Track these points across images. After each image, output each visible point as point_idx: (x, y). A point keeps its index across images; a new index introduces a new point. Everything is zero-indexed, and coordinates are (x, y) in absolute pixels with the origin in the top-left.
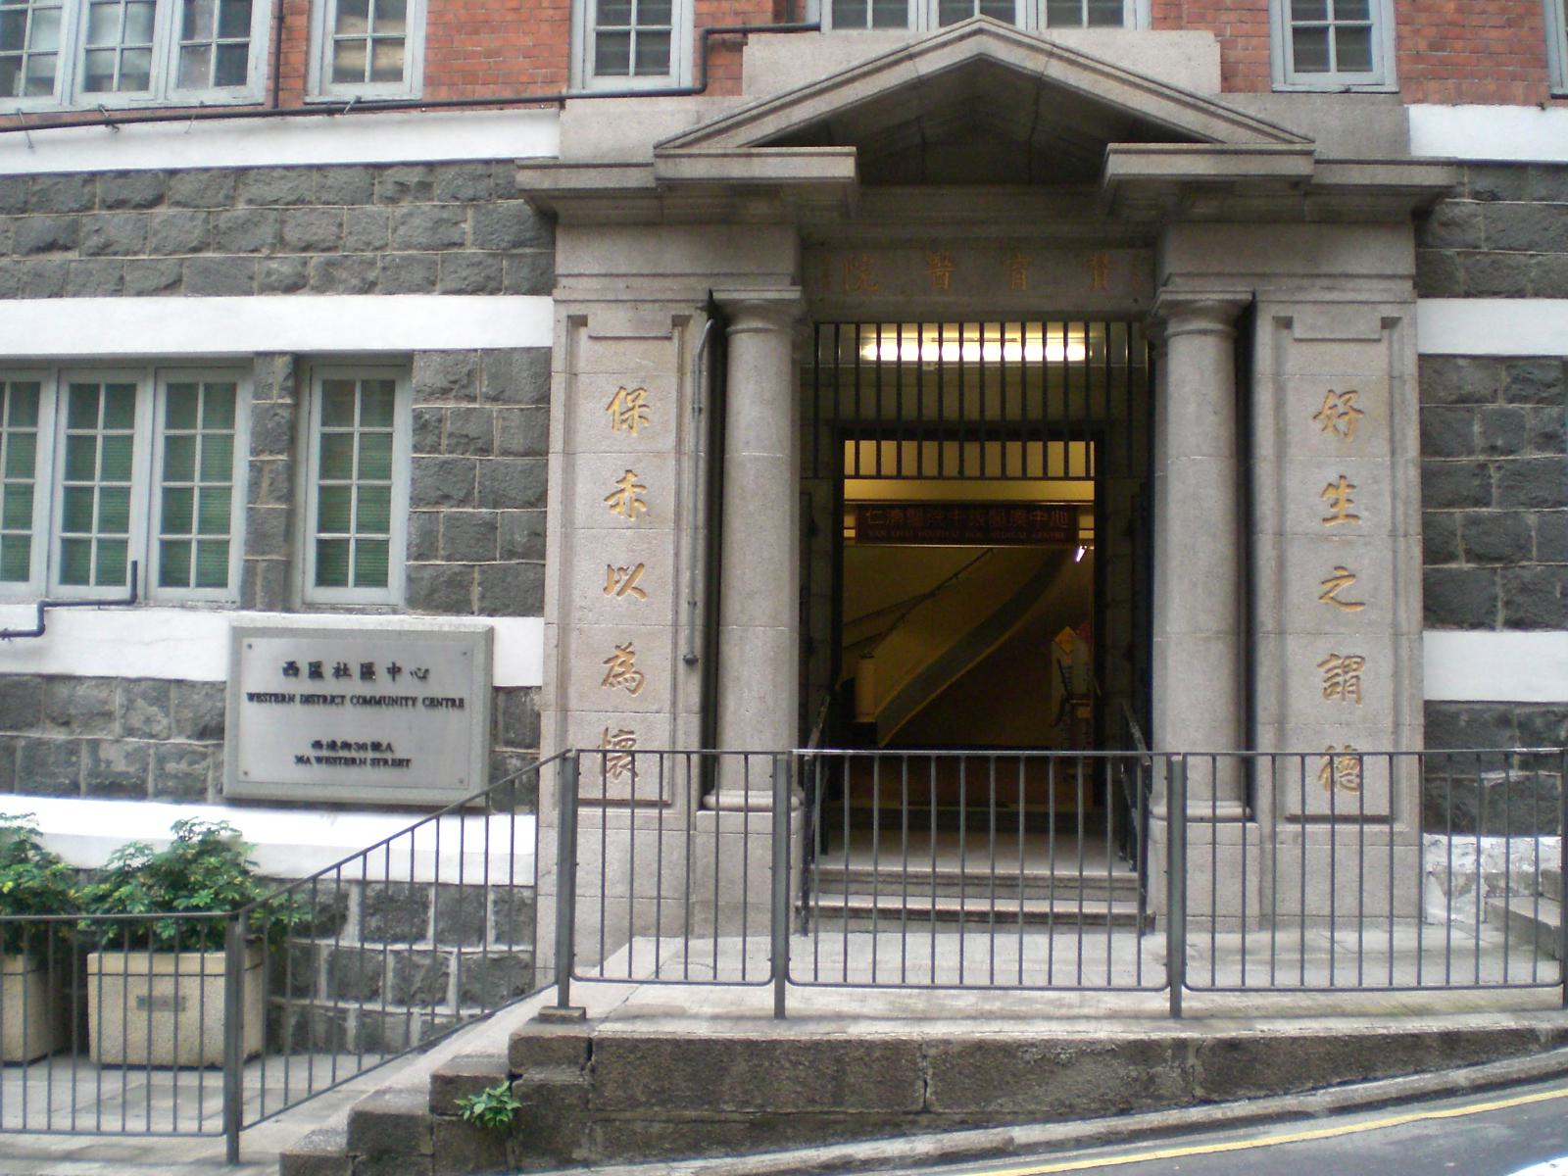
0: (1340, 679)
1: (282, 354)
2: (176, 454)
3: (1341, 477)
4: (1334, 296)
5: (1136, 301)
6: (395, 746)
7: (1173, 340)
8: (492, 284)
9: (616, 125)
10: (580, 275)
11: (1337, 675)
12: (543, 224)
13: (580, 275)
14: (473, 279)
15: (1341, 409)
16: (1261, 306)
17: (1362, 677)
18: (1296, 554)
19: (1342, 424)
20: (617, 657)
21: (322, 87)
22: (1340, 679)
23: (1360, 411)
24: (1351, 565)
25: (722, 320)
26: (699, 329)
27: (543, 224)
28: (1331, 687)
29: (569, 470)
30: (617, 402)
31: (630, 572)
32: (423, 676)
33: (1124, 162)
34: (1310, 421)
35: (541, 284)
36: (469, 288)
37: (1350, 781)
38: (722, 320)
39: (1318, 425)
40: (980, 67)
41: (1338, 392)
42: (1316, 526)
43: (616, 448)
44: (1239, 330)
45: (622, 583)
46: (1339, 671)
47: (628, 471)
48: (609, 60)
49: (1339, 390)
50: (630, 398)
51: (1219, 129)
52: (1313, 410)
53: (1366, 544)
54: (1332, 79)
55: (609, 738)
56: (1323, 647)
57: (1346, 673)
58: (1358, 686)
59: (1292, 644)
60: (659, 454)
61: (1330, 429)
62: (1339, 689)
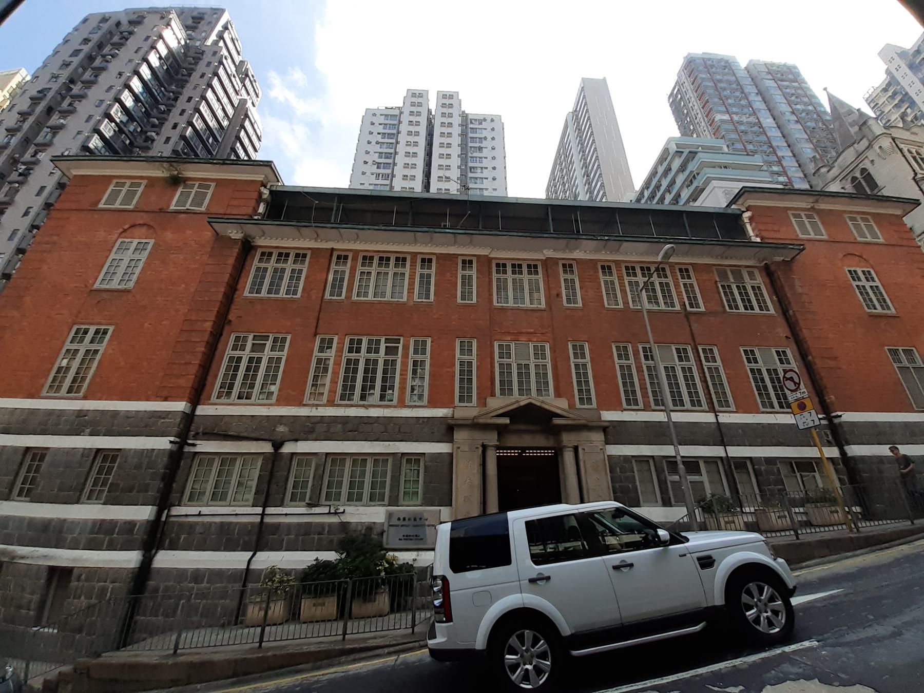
2: (374, 475)
9: (468, 411)
12: (447, 430)
21: (407, 403)
25: (485, 447)
26: (481, 449)
27: (447, 430)
29: (457, 477)
33: (557, 421)
35: (451, 440)
40: (530, 404)
48: (461, 399)
51: (571, 416)
54: (586, 406)
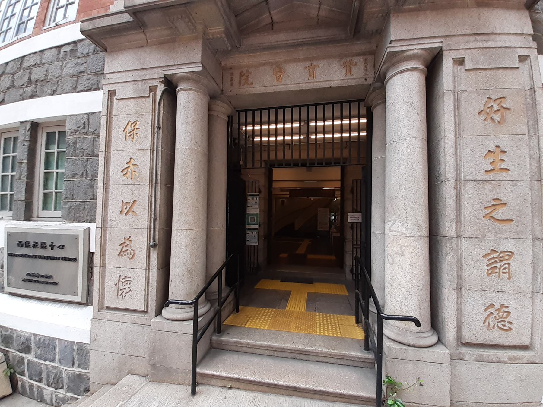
0: (498, 265)
1: (27, 121)
3: (498, 147)
4: (490, 44)
5: (366, 80)
6: (54, 277)
7: (392, 81)
8: (95, 87)
10: (114, 73)
11: (496, 262)
13: (114, 73)
14: (87, 85)
15: (496, 107)
16: (445, 53)
17: (512, 264)
18: (470, 194)
19: (497, 117)
20: (125, 242)
22: (498, 265)
23: (507, 109)
24: (504, 199)
28: (492, 269)
30: (127, 128)
31: (131, 204)
32: (62, 247)
34: (477, 115)
36: (86, 89)
37: (504, 326)
38: (171, 87)
39: (482, 118)
41: (494, 98)
42: (481, 176)
43: (126, 148)
44: (432, 67)
45: (127, 209)
46: (497, 260)
47: (130, 158)
49: (494, 97)
50: (133, 125)
52: (477, 110)
53: (513, 186)
55: (121, 280)
56: (486, 246)
57: (502, 261)
58: (509, 269)
59: (465, 244)
60: (143, 150)
61: (489, 121)
62: (497, 270)
